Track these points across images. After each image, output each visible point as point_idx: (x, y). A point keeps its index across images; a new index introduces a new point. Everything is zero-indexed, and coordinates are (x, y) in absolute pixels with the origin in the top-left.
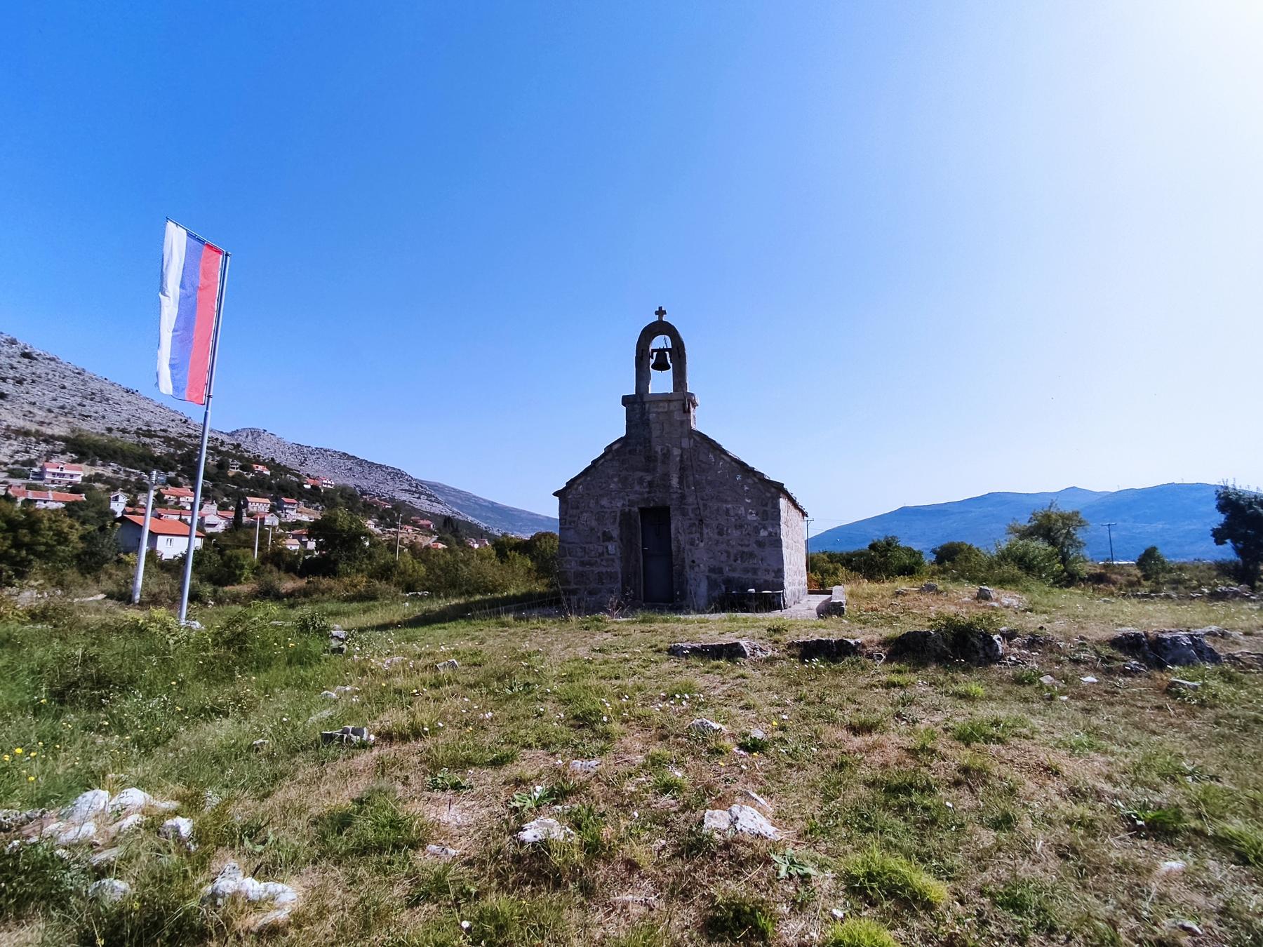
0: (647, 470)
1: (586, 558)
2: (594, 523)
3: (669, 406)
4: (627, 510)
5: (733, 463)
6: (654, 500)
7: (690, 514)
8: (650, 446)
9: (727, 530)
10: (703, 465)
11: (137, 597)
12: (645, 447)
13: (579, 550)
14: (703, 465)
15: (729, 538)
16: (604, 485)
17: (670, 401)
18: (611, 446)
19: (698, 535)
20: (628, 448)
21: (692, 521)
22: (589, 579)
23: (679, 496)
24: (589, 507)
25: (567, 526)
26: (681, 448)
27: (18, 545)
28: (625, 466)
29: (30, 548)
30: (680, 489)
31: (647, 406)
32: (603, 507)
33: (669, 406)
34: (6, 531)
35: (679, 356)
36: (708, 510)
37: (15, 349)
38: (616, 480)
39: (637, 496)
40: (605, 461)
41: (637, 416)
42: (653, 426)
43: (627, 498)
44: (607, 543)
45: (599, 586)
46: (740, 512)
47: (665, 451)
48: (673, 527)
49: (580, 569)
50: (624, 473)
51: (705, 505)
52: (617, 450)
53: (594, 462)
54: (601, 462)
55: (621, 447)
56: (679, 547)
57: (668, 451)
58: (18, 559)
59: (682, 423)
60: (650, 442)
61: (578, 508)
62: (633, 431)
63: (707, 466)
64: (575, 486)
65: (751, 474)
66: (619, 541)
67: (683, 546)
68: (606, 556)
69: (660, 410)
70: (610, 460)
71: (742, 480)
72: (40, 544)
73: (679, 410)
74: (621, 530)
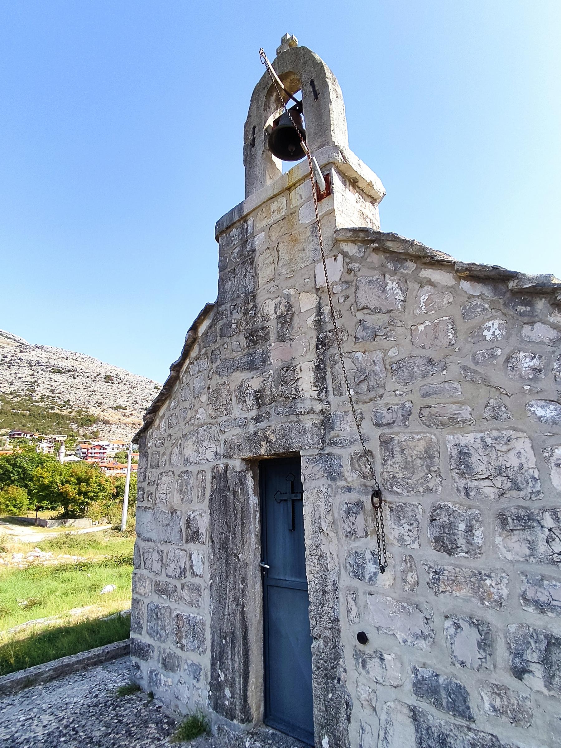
0: (251, 366)
1: (162, 578)
2: (176, 498)
3: (288, 201)
4: (221, 467)
5: (466, 285)
6: (266, 438)
7: (346, 469)
8: (255, 306)
9: (470, 530)
10: (372, 320)
11: (124, 527)
12: (246, 313)
13: (156, 556)
14: (372, 320)
15: (478, 564)
16: (190, 413)
17: (289, 189)
18: (194, 328)
19: (372, 543)
20: (220, 324)
21: (354, 497)
22: (163, 627)
23: (317, 419)
24: (171, 464)
25: (144, 504)
26: (318, 290)
27: (80, 493)
28: (215, 366)
29: (85, 494)
30: (320, 400)
31: (250, 223)
32: (187, 461)
33: (288, 201)
34: (76, 484)
35: (316, 98)
36: (398, 457)
37: (152, 386)
38: (204, 398)
39: (238, 430)
40: (191, 363)
41: (236, 250)
42: (260, 260)
43: (223, 437)
44: (191, 546)
45: (179, 652)
46: (513, 461)
47: (283, 309)
48: (307, 510)
49: (156, 600)
50: (216, 380)
51: (386, 443)
52: (206, 334)
53: (176, 368)
54: (185, 367)
55: (210, 327)
56: (324, 580)
57: (289, 306)
58: (80, 501)
59: (315, 226)
60: (254, 297)
61: (157, 466)
62: (228, 285)
63: (382, 319)
64: (157, 423)
65: (541, 304)
66: (209, 544)
67: (332, 577)
68: (189, 579)
69: (272, 220)
70: (197, 358)
71: (507, 338)
72: (91, 492)
73: (309, 199)
74: (212, 519)
